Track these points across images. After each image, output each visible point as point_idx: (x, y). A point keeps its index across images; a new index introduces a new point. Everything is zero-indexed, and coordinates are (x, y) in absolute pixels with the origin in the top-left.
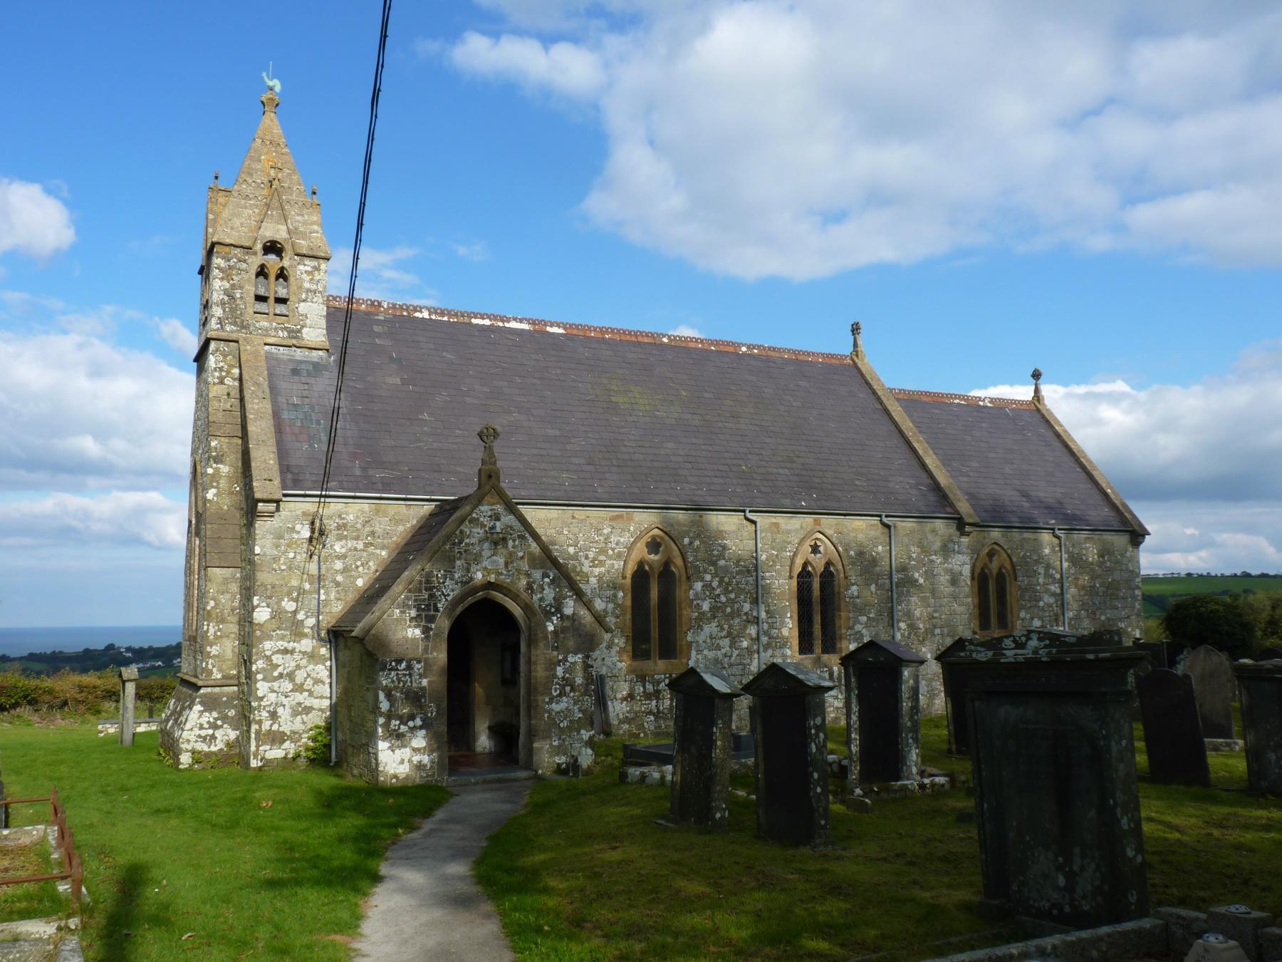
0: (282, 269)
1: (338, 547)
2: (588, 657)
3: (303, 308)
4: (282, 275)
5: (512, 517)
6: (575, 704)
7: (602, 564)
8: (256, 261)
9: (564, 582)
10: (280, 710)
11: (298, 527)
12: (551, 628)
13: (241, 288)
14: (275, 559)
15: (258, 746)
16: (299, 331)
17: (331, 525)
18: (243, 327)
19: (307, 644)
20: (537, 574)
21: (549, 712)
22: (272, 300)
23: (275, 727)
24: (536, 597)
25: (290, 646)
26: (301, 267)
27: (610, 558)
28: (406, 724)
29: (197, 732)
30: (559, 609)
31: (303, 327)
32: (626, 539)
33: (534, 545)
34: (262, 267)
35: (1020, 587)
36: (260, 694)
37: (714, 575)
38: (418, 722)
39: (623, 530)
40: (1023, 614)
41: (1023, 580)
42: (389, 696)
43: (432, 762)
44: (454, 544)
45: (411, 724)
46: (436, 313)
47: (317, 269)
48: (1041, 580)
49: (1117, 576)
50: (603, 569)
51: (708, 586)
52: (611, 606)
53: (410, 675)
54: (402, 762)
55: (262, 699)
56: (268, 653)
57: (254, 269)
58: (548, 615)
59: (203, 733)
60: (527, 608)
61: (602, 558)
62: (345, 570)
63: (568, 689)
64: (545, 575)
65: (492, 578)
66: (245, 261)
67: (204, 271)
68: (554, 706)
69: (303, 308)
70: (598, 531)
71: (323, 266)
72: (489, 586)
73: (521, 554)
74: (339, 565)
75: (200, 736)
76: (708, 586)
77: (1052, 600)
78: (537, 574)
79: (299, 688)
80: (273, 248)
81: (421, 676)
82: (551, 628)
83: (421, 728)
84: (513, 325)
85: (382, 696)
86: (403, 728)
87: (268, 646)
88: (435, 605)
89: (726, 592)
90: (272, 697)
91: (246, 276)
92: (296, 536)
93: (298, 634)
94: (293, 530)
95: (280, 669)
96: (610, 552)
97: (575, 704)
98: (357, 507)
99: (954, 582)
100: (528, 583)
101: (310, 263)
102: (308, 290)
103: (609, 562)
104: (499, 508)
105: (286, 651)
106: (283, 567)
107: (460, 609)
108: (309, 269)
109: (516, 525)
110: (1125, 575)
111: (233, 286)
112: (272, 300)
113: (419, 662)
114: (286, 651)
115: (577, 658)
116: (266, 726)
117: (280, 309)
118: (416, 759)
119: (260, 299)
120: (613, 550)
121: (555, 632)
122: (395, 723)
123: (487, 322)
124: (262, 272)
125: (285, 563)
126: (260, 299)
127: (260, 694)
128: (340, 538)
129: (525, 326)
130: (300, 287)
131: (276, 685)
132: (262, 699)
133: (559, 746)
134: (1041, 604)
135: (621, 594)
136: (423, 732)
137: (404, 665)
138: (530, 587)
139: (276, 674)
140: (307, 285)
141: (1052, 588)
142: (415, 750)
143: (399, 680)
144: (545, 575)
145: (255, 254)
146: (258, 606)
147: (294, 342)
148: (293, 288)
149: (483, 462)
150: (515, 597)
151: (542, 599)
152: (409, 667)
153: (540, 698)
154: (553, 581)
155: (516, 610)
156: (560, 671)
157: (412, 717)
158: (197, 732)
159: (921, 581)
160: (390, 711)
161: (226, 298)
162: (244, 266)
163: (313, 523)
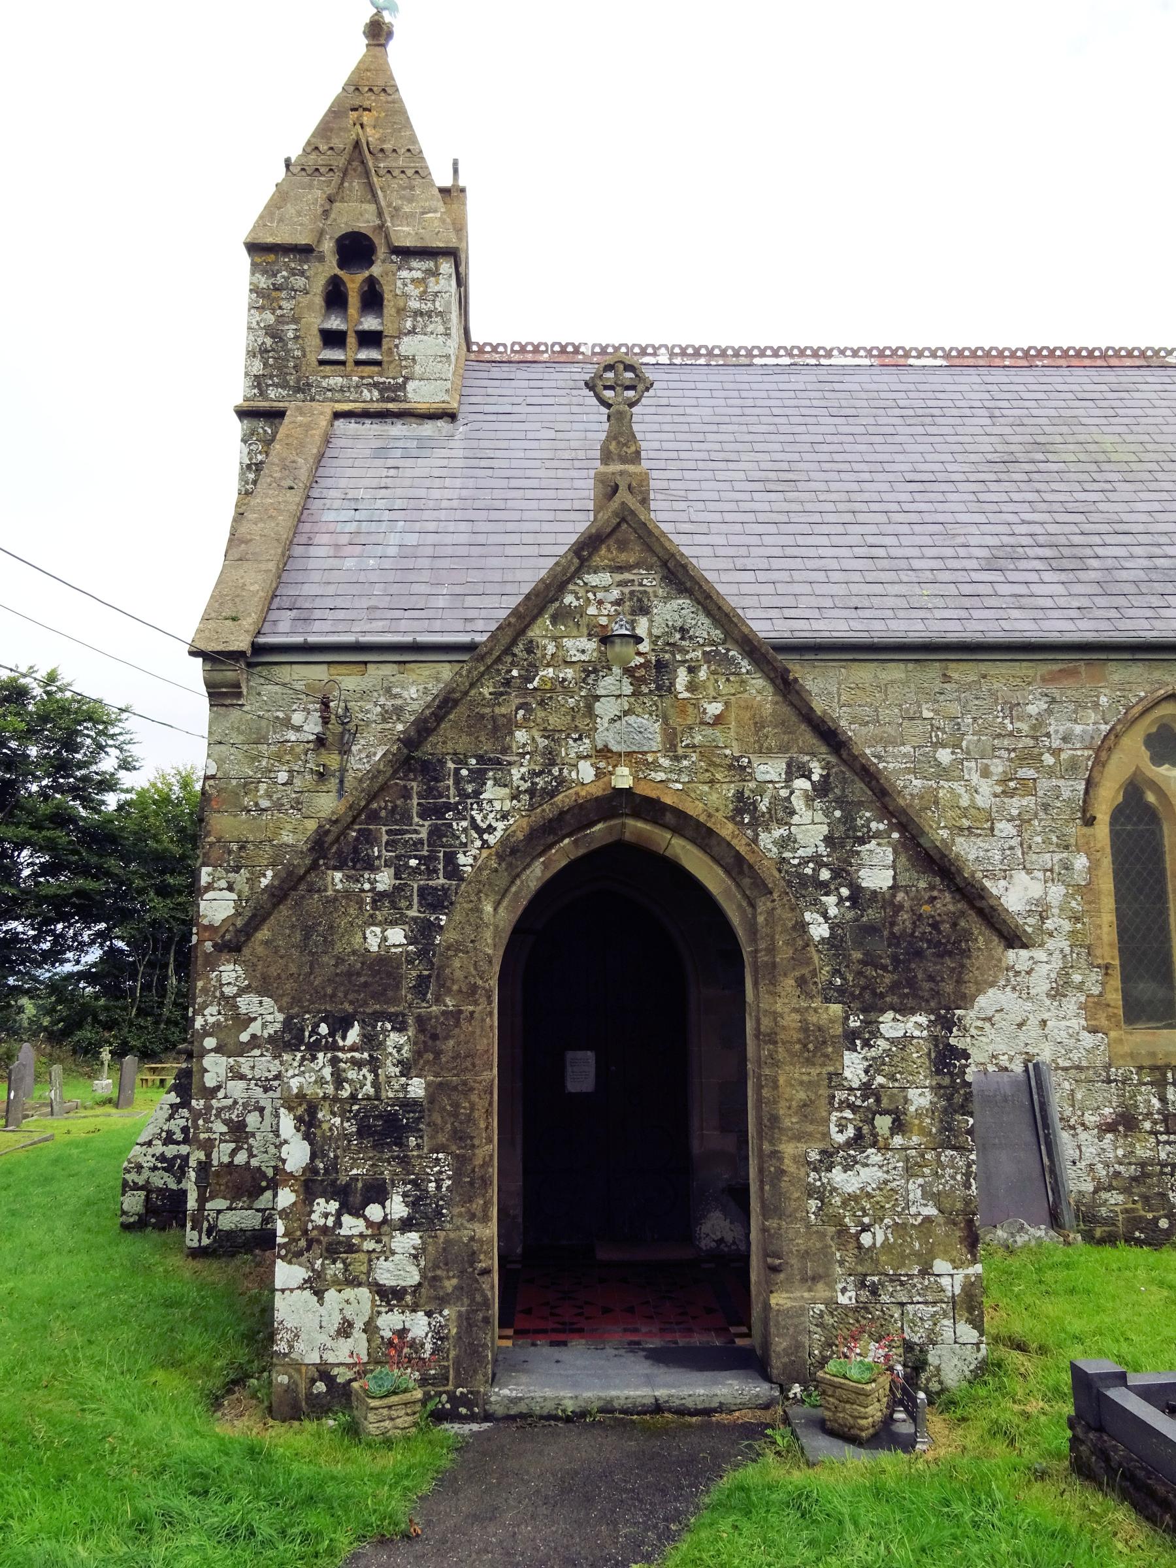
0: (372, 282)
2: (948, 1024)
3: (408, 346)
4: (373, 299)
5: (684, 602)
6: (910, 1171)
7: (1027, 787)
9: (858, 790)
10: (252, 1120)
11: (297, 718)
12: (819, 930)
13: (295, 320)
14: (248, 786)
15: (202, 1200)
16: (403, 387)
18: (298, 390)
20: (770, 770)
21: (821, 1194)
22: (351, 340)
23: (241, 1158)
24: (766, 840)
26: (404, 274)
27: (1050, 773)
28: (358, 1212)
29: (159, 1148)
30: (843, 873)
31: (407, 379)
32: (1090, 725)
33: (758, 683)
36: (210, 1081)
38: (397, 1208)
39: (1080, 705)
42: (308, 1124)
43: (439, 1335)
44: (508, 683)
45: (374, 1212)
46: (683, 353)
47: (435, 273)
50: (1028, 801)
52: (1056, 892)
53: (374, 1065)
54: (345, 1329)
55: (212, 1092)
56: (229, 991)
57: (319, 286)
58: (806, 887)
59: (171, 1151)
60: (737, 866)
61: (1027, 773)
63: (883, 1123)
64: (797, 770)
65: (623, 778)
66: (302, 273)
68: (837, 1176)
69: (408, 346)
70: (1013, 709)
72: (619, 802)
73: (714, 709)
75: (162, 1158)
78: (770, 770)
80: (355, 249)
81: (406, 1069)
82: (819, 930)
83: (406, 1225)
85: (287, 1124)
86: (351, 1226)
88: (450, 858)
90: (237, 1088)
91: (304, 300)
92: (292, 736)
94: (287, 723)
95: (255, 1028)
96: (1049, 759)
97: (910, 1171)
98: (426, 671)
100: (739, 796)
101: (418, 267)
102: (418, 313)
103: (1044, 784)
104: (650, 581)
106: (265, 803)
107: (535, 875)
108: (418, 275)
109: (703, 628)
111: (280, 320)
112: (351, 340)
113: (400, 1028)
115: (916, 1024)
116: (222, 1153)
118: (390, 1322)
120: (1056, 752)
121: (834, 942)
122: (324, 1208)
124: (335, 298)
125: (269, 796)
126: (333, 339)
127: (210, 1081)
130: (401, 311)
131: (245, 1065)
132: (212, 1092)
133: (861, 1308)
135: (1081, 862)
136: (413, 1238)
137: (354, 1035)
138: (743, 805)
139: (244, 1037)
140: (414, 304)
142: (390, 1296)
143: (339, 1080)
144: (797, 770)
145: (321, 259)
146: (209, 887)
147: (390, 406)
148: (389, 309)
149: (606, 457)
151: (786, 842)
152: (370, 1041)
153: (789, 1149)
154: (822, 789)
156: (853, 1067)
157: (378, 1192)
158: (159, 1148)
160: (311, 1169)
161: (269, 341)
162: (299, 282)
163: (325, 704)
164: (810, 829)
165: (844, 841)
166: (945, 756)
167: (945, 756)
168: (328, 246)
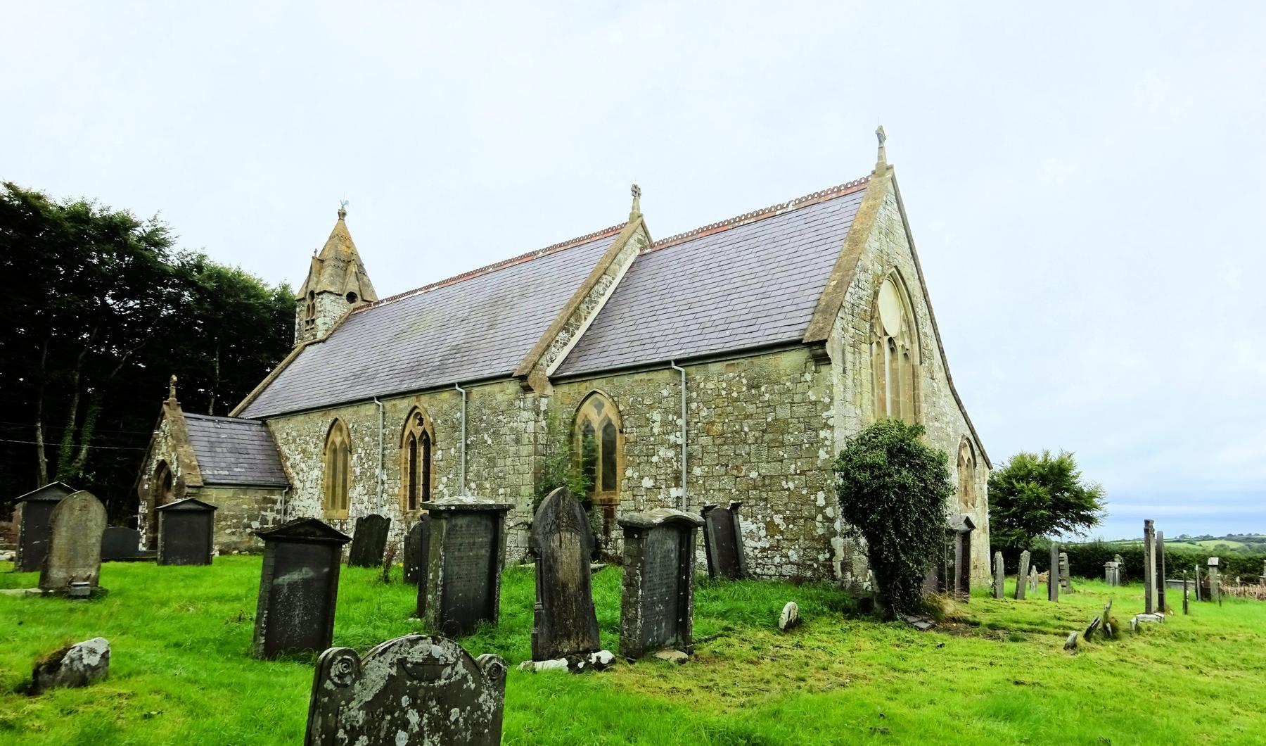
35: (627, 441)
37: (363, 448)
40: (629, 473)
41: (632, 433)
48: (656, 430)
49: (784, 412)
76: (360, 458)
77: (671, 454)
89: (368, 460)
99: (517, 441)
110: (801, 410)
134: (655, 459)
141: (672, 438)
159: (489, 442)
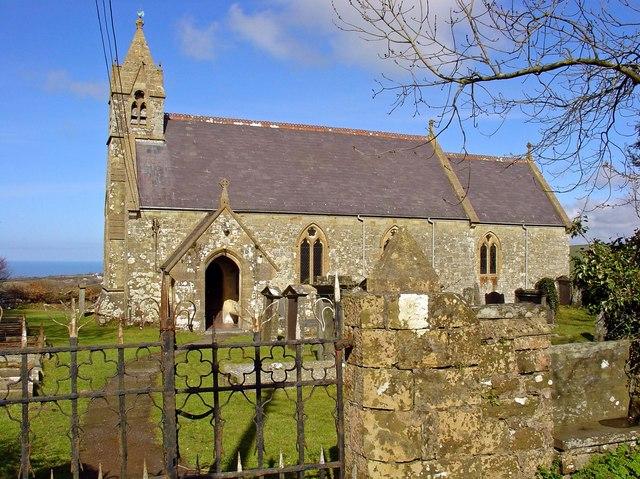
1: (164, 231)
4: (143, 106)
8: (132, 99)
17: (161, 221)
19: (151, 274)
25: (144, 274)
34: (135, 103)
51: (338, 251)
62: (168, 241)
65: (224, 247)
67: (108, 143)
70: (285, 225)
71: (162, 101)
72: (225, 251)
74: (164, 239)
76: (338, 251)
79: (147, 293)
80: (139, 94)
84: (254, 125)
87: (134, 274)
93: (147, 270)
94: (144, 224)
105: (141, 277)
114: (141, 277)
117: (143, 122)
119: (133, 117)
123: (241, 124)
124: (134, 106)
126: (133, 117)
128: (165, 227)
129: (259, 125)
135: (295, 254)
150: (236, 256)
155: (237, 262)
164: (251, 254)
165: (255, 256)
166: (271, 233)
167: (271, 233)
168: (133, 93)
